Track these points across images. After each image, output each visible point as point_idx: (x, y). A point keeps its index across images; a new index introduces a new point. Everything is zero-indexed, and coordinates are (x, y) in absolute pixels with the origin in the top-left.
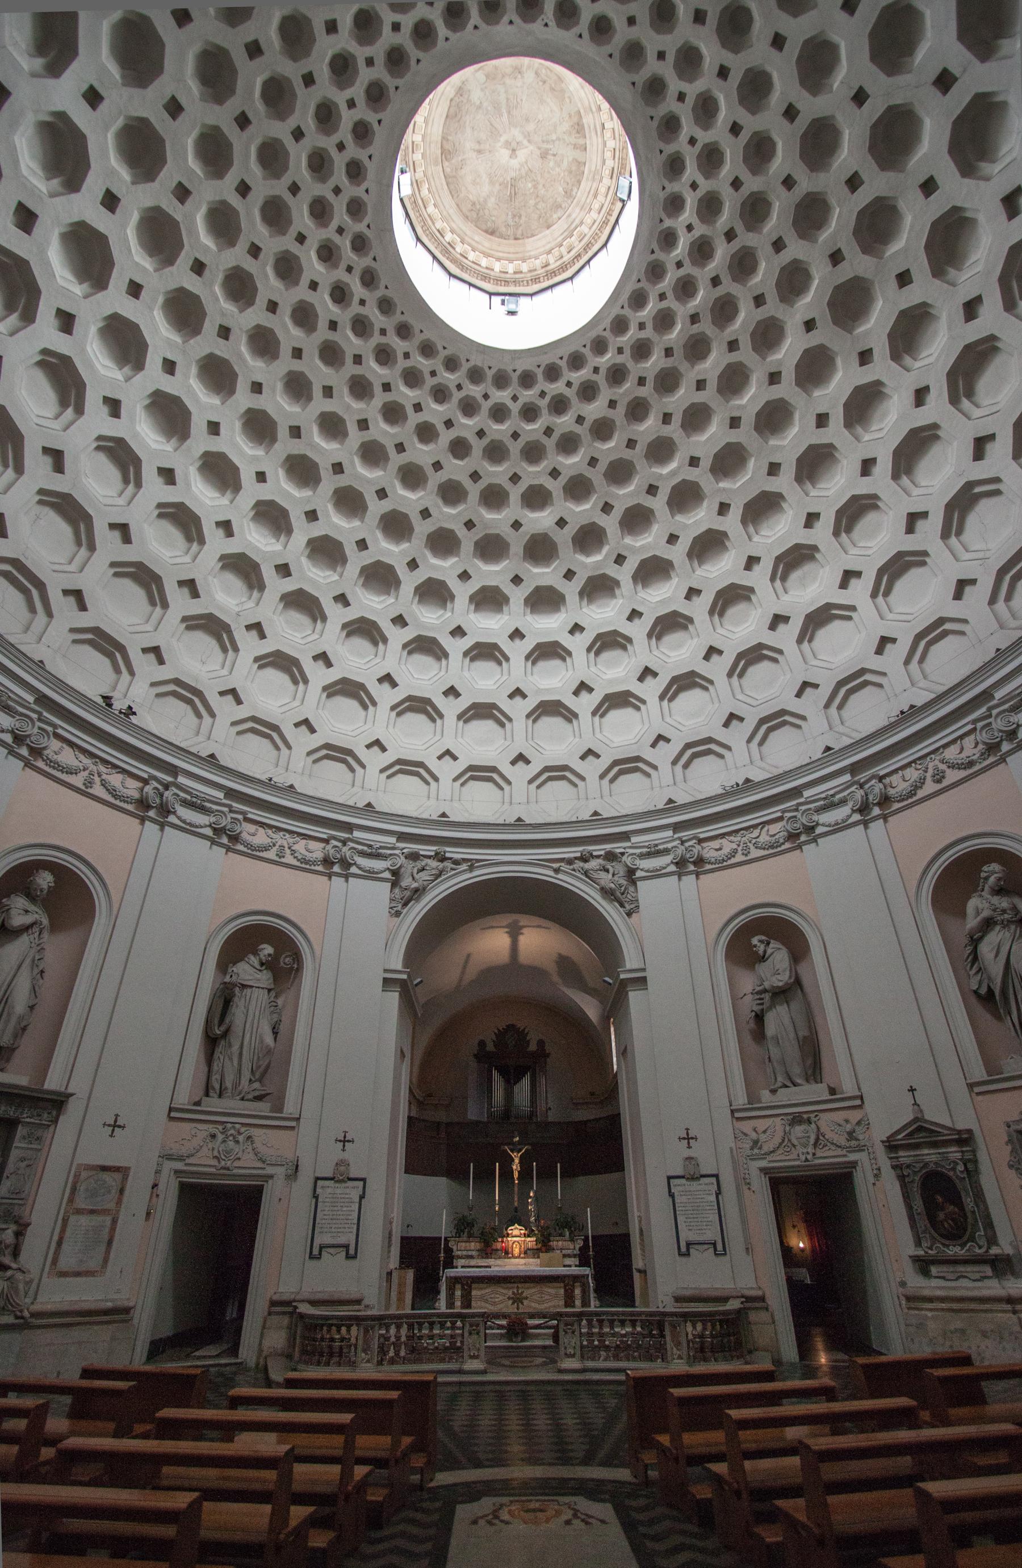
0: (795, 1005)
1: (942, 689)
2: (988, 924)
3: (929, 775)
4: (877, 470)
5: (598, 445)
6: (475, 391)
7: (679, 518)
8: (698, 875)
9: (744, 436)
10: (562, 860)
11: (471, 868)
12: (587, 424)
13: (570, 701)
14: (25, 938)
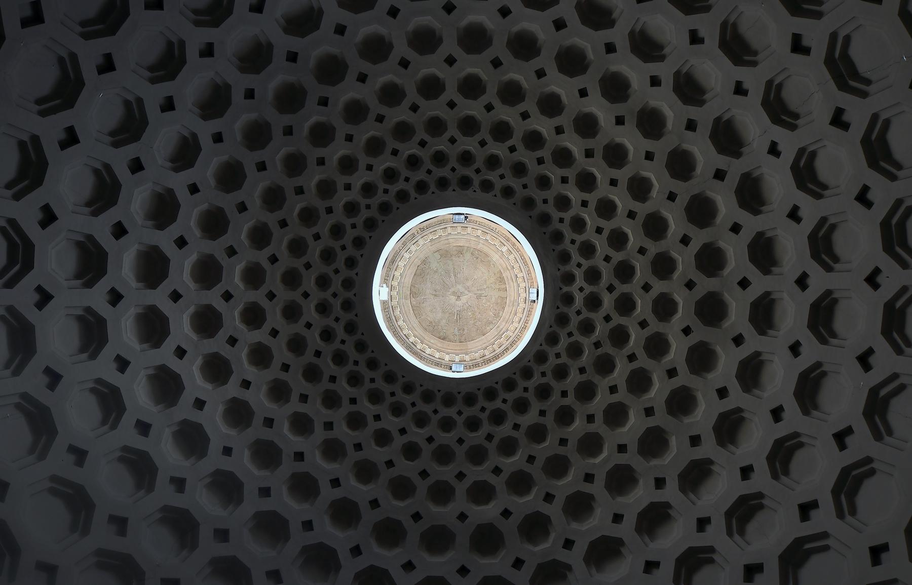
7: (620, 499)
9: (661, 419)
12: (523, 430)
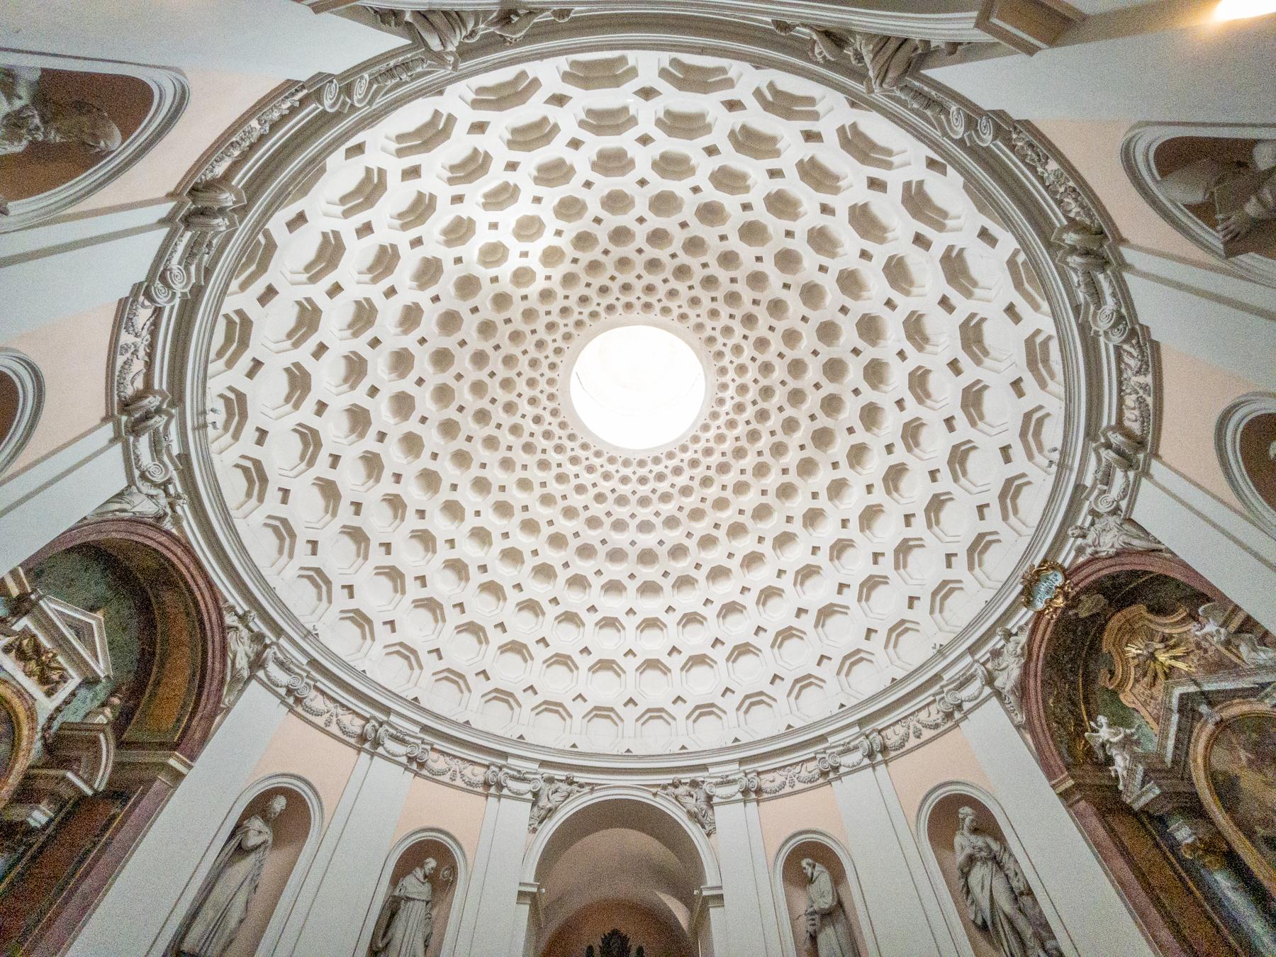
0: (840, 928)
1: (912, 669)
2: (971, 860)
3: (911, 731)
4: (850, 525)
5: (683, 499)
6: (611, 468)
7: (734, 543)
8: (758, 802)
9: (771, 499)
10: (658, 786)
11: (592, 790)
12: (677, 488)
13: (665, 660)
14: (251, 859)
